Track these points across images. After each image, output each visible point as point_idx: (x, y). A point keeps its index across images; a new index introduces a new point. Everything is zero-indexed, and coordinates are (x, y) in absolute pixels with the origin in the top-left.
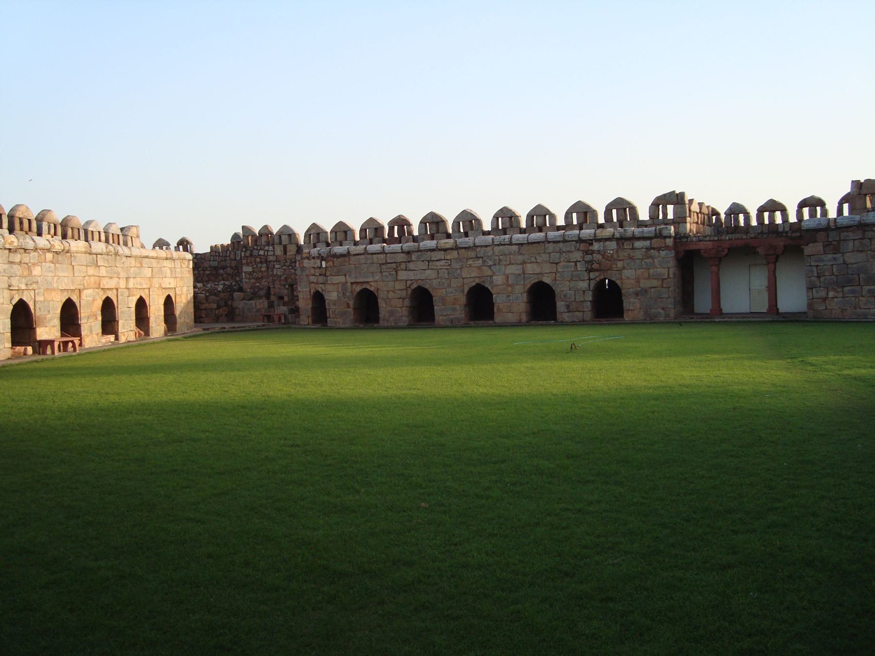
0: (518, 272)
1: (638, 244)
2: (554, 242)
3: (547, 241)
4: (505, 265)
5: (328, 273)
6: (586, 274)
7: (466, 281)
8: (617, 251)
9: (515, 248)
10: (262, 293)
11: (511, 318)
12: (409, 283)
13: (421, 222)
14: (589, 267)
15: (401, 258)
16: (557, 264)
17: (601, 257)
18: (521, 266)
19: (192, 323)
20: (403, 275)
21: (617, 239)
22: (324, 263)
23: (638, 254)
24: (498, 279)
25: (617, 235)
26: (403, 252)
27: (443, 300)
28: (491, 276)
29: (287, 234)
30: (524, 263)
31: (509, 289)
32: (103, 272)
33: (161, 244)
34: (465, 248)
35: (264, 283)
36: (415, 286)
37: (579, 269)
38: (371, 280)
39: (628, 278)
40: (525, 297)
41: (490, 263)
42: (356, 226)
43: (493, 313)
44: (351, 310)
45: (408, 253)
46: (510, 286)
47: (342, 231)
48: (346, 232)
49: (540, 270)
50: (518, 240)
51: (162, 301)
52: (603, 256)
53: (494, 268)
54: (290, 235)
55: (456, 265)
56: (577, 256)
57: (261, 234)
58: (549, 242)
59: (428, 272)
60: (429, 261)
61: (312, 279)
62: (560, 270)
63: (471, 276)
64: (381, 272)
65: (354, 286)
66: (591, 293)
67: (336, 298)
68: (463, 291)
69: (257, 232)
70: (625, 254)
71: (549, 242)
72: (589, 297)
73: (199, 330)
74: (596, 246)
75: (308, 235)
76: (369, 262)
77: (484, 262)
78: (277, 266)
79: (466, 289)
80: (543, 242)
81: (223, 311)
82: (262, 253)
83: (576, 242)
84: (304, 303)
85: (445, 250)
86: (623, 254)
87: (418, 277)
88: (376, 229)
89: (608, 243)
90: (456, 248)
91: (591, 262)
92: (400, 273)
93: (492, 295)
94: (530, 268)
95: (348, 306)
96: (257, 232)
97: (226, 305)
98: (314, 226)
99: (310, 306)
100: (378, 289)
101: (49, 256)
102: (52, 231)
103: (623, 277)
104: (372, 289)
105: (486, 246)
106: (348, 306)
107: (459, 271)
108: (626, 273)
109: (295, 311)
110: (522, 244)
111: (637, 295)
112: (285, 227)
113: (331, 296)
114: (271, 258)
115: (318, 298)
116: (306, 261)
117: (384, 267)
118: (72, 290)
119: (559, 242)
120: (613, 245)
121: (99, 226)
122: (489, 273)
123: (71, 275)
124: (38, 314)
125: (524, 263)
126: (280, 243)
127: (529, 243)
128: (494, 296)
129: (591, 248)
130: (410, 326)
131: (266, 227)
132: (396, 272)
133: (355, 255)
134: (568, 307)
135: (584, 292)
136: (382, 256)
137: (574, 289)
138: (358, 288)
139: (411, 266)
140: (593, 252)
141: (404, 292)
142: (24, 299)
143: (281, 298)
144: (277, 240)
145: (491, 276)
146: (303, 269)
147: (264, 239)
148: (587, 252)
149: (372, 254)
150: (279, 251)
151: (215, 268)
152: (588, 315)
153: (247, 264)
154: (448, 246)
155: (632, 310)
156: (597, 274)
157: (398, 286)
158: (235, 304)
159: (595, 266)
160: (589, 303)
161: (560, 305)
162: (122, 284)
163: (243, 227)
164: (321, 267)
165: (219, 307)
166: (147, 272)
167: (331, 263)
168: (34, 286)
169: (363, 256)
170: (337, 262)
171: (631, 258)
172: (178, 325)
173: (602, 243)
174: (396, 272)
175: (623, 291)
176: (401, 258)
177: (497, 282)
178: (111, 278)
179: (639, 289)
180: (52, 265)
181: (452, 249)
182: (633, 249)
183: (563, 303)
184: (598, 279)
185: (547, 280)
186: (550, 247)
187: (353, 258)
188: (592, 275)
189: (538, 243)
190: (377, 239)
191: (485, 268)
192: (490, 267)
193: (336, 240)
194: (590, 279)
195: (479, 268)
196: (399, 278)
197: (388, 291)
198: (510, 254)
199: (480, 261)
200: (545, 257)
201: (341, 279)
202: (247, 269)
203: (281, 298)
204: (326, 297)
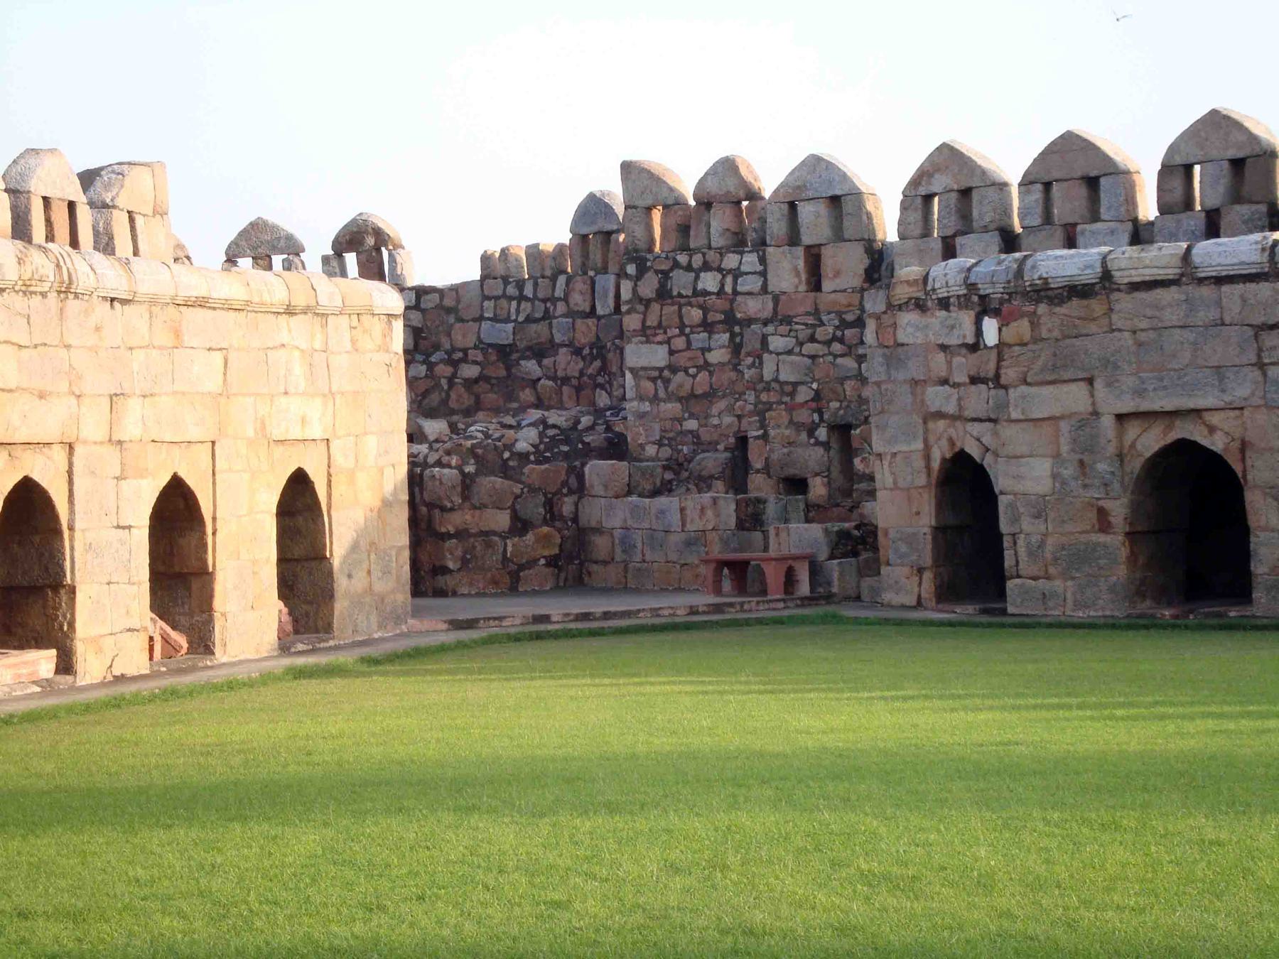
5: (1009, 374)
10: (712, 462)
19: (403, 596)
22: (990, 328)
29: (827, 196)
33: (261, 244)
35: (722, 418)
42: (1141, 153)
44: (1115, 541)
47: (1077, 178)
48: (1092, 183)
51: (270, 499)
54: (835, 201)
57: (705, 203)
61: (937, 397)
64: (1261, 366)
65: (1132, 430)
69: (687, 188)
73: (430, 627)
75: (918, 198)
78: (777, 343)
82: (709, 282)
84: (903, 508)
88: (1238, 165)
95: (1103, 521)
96: (687, 188)
97: (552, 515)
98: (947, 158)
99: (927, 519)
100: (1244, 446)
104: (1216, 443)
106: (1103, 521)
109: (859, 543)
112: (815, 165)
113: (1025, 476)
114: (753, 307)
115: (966, 488)
116: (908, 319)
126: (793, 239)
131: (728, 166)
133: (1135, 287)
138: (1151, 441)
142: (36, 477)
143: (797, 485)
144: (777, 226)
146: (895, 351)
147: (719, 222)
149: (1220, 280)
150: (786, 271)
151: (504, 352)
153: (646, 333)
158: (593, 512)
162: (93, 427)
163: (628, 169)
164: (975, 347)
165: (520, 526)
166: (205, 372)
167: (1021, 328)
169: (1172, 294)
170: (1051, 318)
172: (340, 606)
178: (42, 396)
187: (1124, 303)
190: (1244, 210)
193: (1048, 219)
201: (1073, 398)
202: (644, 355)
203: (797, 485)
204: (1002, 480)
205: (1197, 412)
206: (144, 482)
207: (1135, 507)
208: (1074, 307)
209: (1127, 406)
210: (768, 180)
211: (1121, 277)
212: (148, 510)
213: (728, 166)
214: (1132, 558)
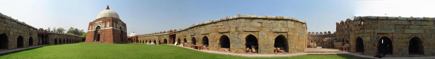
12: (410, 35)
27: (429, 45)
36: (412, 37)
38: (389, 32)
64: (395, 29)
65: (379, 35)
67: (369, 40)
100: (392, 38)
104: (389, 37)
113: (366, 39)
117: (397, 26)
157: (404, 36)
169: (386, 21)
187: (379, 21)
196: (405, 32)
197: (399, 39)
204: (364, 39)
205: (387, 33)
208: (374, 21)
209: (379, 32)
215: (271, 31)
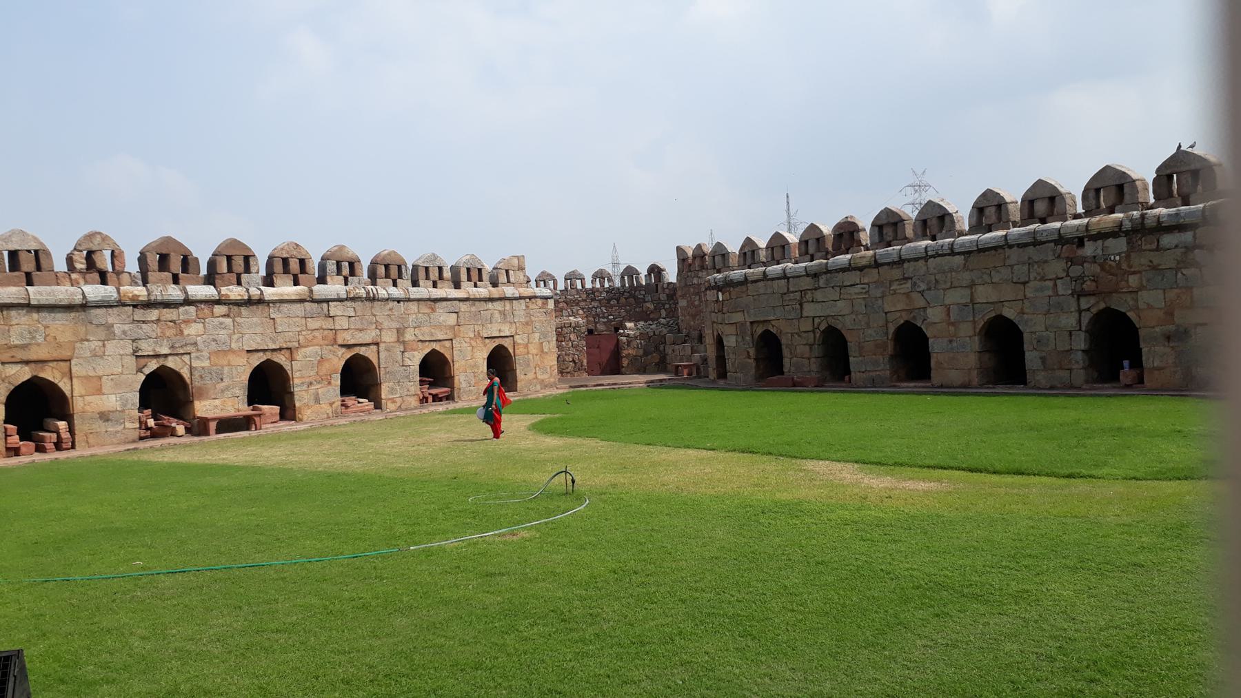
0: (963, 301)
1: (1167, 240)
2: (1019, 246)
3: (1006, 244)
4: (945, 290)
5: (725, 310)
6: (1073, 301)
7: (891, 317)
8: (1128, 257)
9: (959, 260)
10: (695, 334)
11: (955, 376)
12: (817, 320)
13: (873, 225)
14: (1078, 289)
15: (807, 283)
16: (1024, 283)
17: (1098, 269)
18: (968, 291)
20: (809, 310)
21: (1127, 233)
23: (1167, 260)
24: (935, 314)
25: (1127, 225)
26: (808, 275)
28: (925, 309)
30: (972, 285)
31: (952, 328)
32: (342, 323)
34: (888, 264)
36: (822, 327)
37: (1061, 291)
39: (1150, 307)
40: (976, 343)
41: (923, 286)
43: (930, 369)
44: (751, 361)
45: (815, 275)
46: (953, 324)
49: (995, 296)
50: (963, 245)
52: (1102, 267)
53: (929, 295)
55: (877, 292)
56: (1057, 268)
57: (694, 257)
58: (1010, 247)
59: (839, 304)
60: (841, 287)
62: (1029, 295)
63: (896, 308)
65: (755, 325)
66: (1082, 335)
68: (887, 333)
69: (690, 253)
70: (1144, 261)
71: (1010, 247)
72: (1080, 342)
74: (1089, 249)
76: (769, 291)
77: (914, 284)
79: (892, 329)
80: (1001, 247)
81: (656, 357)
82: (695, 281)
83: (1056, 242)
85: (861, 269)
86: (1139, 261)
87: (828, 312)
88: (818, 240)
89: (1110, 242)
90: (876, 264)
91: (1080, 279)
92: (806, 306)
93: (927, 339)
94: (984, 293)
97: (657, 348)
101: (219, 310)
102: (346, 271)
103: (1141, 305)
105: (916, 260)
106: (749, 357)
107: (880, 301)
108: (1145, 297)
110: (969, 253)
111: (1168, 338)
117: (786, 297)
118: (274, 350)
119: (1025, 245)
120: (1120, 244)
121: (448, 262)
122: (922, 303)
123: (269, 331)
124: (197, 383)
125: (972, 285)
127: (980, 251)
128: (931, 341)
129: (1080, 252)
130: (819, 385)
131: (699, 246)
132: (801, 305)
134: (1043, 359)
135: (1070, 332)
136: (783, 282)
137: (1053, 327)
139: (819, 295)
140: (1083, 261)
141: (811, 335)
145: (925, 309)
147: (697, 262)
148: (1072, 261)
149: (773, 279)
152: (1079, 376)
153: (683, 296)
154: (864, 263)
155: (1159, 369)
156: (1092, 300)
159: (1089, 286)
160: (1080, 356)
161: (1032, 358)
164: (717, 301)
166: (452, 320)
168: (188, 349)
169: (761, 284)
170: (735, 291)
171: (1154, 268)
172: (519, 384)
173: (1100, 242)
174: (801, 305)
175: (1142, 333)
176: (807, 283)
177: (933, 320)
179: (1172, 328)
180: (228, 321)
181: (869, 266)
182: (1158, 249)
183: (1035, 353)
184: (1094, 310)
185: (1009, 313)
186: (1014, 255)
188: (1085, 302)
189: (995, 248)
191: (915, 295)
192: (922, 293)
193: (773, 259)
194: (1080, 312)
195: (907, 295)
198: (952, 270)
199: (909, 285)
200: (1005, 272)
201: (738, 317)
202: (683, 303)
206: (416, 353)
207: (757, 351)
210: (708, 248)
211: (750, 279)
212: (418, 363)
213: (719, 244)
214: (757, 367)
215: (478, 335)
